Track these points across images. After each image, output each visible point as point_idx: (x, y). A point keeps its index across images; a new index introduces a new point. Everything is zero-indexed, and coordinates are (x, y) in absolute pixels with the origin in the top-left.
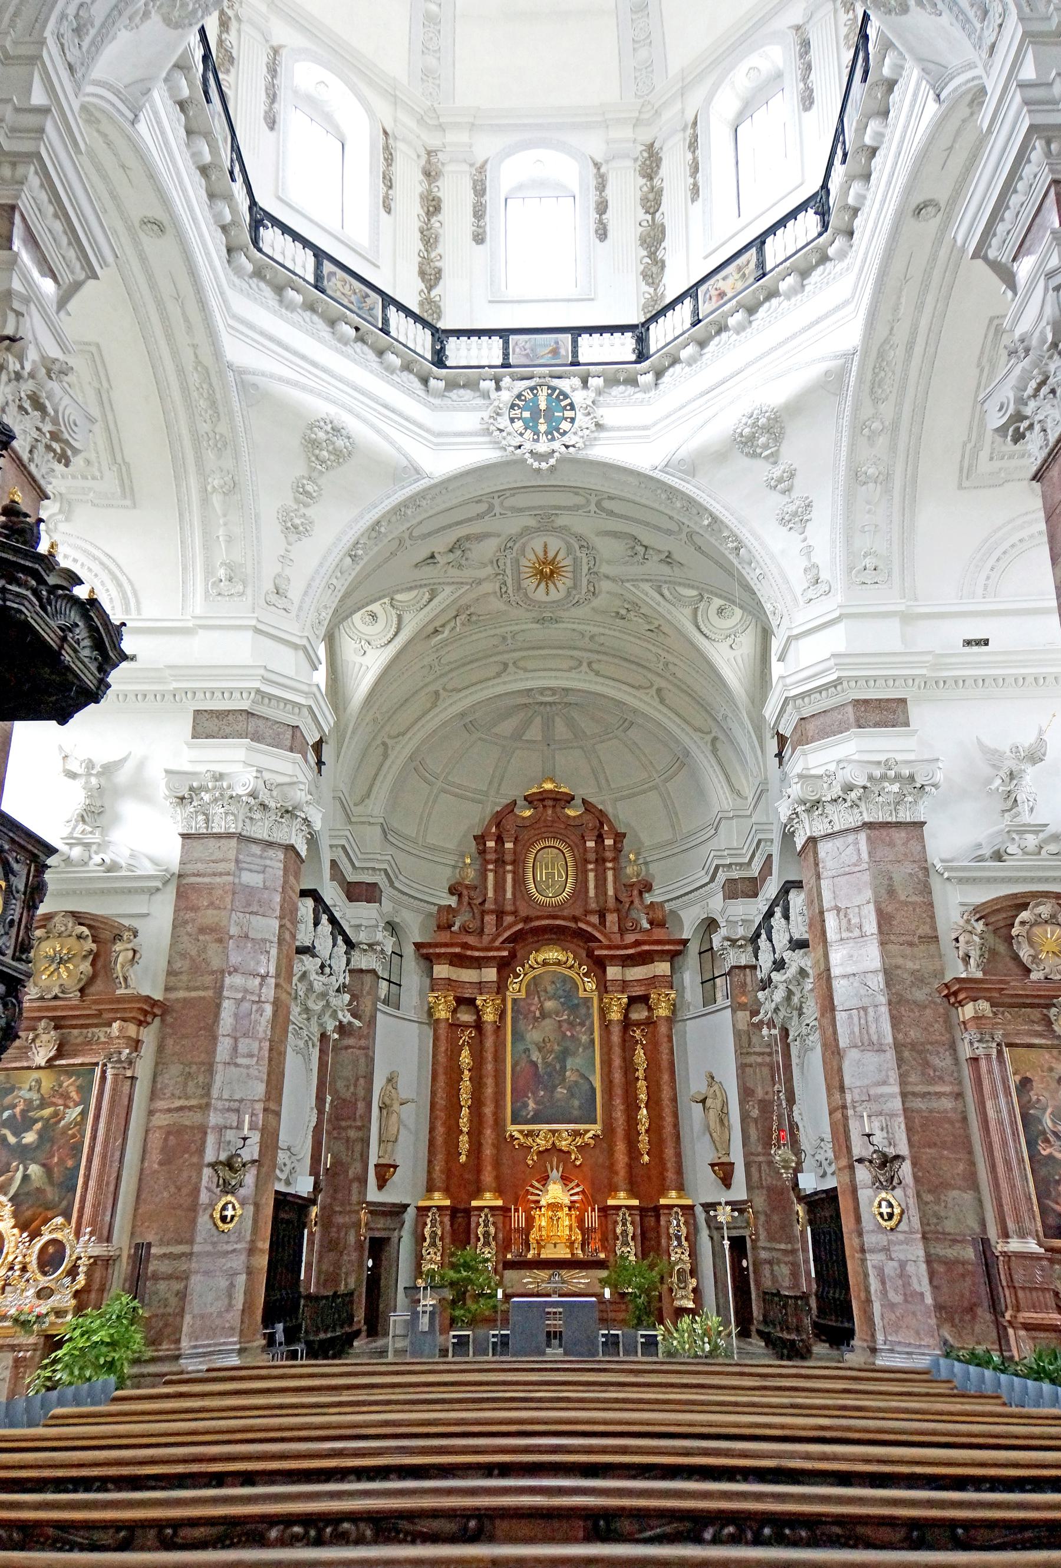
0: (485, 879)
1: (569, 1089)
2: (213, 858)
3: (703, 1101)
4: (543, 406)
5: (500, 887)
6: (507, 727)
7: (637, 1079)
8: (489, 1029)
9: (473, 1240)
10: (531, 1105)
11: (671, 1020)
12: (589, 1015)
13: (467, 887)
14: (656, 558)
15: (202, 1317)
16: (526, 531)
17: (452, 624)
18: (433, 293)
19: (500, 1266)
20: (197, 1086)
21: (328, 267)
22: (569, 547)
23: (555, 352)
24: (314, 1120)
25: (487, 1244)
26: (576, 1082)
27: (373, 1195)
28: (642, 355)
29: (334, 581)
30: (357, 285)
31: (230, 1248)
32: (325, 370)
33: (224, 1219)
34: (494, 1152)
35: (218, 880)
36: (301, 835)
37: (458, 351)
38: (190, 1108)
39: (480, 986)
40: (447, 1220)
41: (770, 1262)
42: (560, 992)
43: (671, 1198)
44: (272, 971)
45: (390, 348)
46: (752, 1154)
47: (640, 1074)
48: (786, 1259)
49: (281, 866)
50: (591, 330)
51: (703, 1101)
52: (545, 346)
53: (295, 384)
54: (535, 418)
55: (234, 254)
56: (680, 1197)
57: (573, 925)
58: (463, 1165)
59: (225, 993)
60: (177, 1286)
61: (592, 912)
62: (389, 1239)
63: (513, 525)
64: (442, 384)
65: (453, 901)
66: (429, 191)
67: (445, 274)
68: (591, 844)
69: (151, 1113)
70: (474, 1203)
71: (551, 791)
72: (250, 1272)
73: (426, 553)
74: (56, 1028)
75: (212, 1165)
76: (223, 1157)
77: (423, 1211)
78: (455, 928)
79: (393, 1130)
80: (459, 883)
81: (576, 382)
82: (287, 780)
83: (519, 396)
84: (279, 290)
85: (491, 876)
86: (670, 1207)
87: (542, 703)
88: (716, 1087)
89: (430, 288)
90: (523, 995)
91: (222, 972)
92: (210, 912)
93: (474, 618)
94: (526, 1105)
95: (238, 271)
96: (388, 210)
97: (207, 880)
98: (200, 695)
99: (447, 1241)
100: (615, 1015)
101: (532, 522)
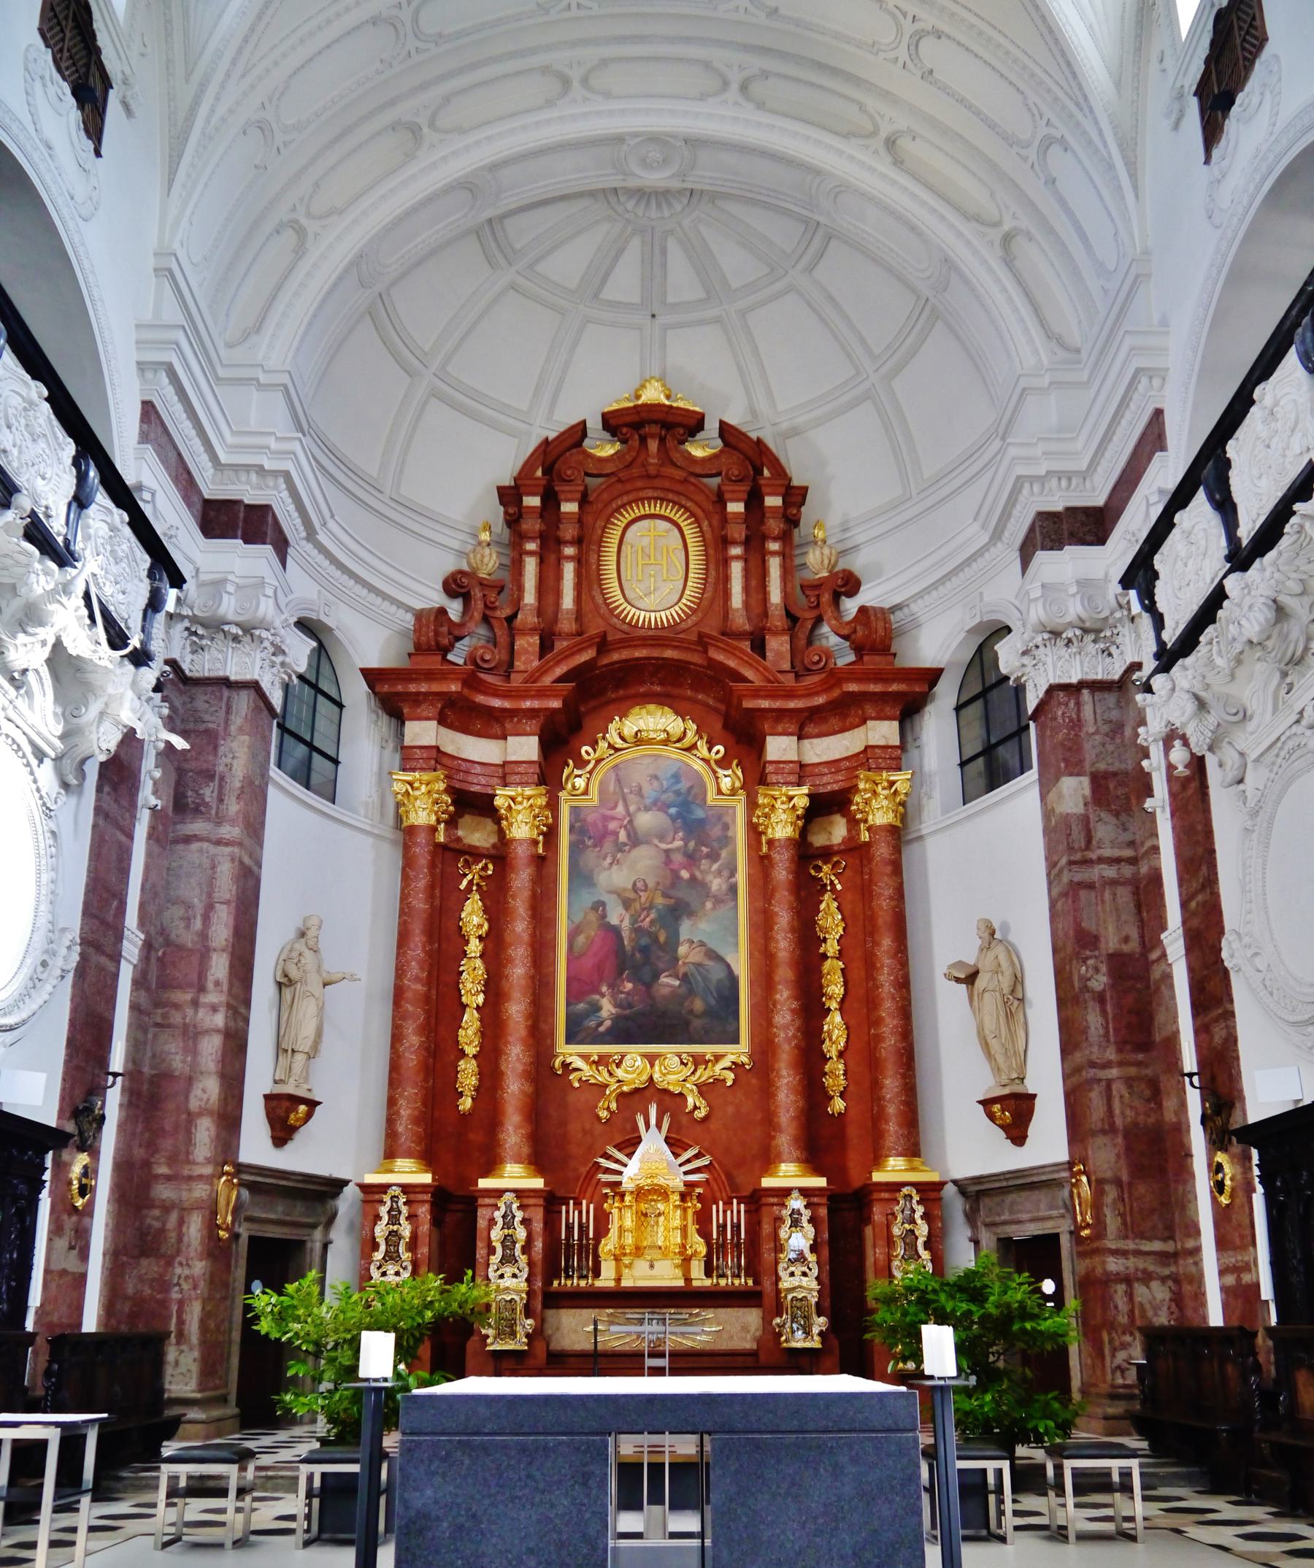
0: (517, 568)
1: (685, 978)
3: (971, 979)
5: (549, 586)
8: (522, 852)
9: (481, 1252)
11: (898, 834)
12: (727, 840)
13: (482, 584)
19: (538, 1304)
25: (508, 1259)
26: (698, 965)
34: (528, 1088)
39: (505, 773)
40: (424, 1211)
41: (1128, 1280)
42: (669, 797)
43: (894, 1169)
46: (1093, 1065)
47: (831, 947)
48: (1166, 1272)
51: (971, 979)
56: (913, 1169)
57: (696, 658)
58: (465, 1117)
61: (740, 635)
62: (303, 1242)
65: (454, 609)
68: (735, 507)
70: (484, 1183)
71: (660, 406)
77: (372, 1193)
79: (306, 1032)
80: (461, 572)
85: (531, 565)
86: (897, 1187)
88: (999, 951)
94: (599, 1009)
99: (424, 1250)
100: (782, 828)
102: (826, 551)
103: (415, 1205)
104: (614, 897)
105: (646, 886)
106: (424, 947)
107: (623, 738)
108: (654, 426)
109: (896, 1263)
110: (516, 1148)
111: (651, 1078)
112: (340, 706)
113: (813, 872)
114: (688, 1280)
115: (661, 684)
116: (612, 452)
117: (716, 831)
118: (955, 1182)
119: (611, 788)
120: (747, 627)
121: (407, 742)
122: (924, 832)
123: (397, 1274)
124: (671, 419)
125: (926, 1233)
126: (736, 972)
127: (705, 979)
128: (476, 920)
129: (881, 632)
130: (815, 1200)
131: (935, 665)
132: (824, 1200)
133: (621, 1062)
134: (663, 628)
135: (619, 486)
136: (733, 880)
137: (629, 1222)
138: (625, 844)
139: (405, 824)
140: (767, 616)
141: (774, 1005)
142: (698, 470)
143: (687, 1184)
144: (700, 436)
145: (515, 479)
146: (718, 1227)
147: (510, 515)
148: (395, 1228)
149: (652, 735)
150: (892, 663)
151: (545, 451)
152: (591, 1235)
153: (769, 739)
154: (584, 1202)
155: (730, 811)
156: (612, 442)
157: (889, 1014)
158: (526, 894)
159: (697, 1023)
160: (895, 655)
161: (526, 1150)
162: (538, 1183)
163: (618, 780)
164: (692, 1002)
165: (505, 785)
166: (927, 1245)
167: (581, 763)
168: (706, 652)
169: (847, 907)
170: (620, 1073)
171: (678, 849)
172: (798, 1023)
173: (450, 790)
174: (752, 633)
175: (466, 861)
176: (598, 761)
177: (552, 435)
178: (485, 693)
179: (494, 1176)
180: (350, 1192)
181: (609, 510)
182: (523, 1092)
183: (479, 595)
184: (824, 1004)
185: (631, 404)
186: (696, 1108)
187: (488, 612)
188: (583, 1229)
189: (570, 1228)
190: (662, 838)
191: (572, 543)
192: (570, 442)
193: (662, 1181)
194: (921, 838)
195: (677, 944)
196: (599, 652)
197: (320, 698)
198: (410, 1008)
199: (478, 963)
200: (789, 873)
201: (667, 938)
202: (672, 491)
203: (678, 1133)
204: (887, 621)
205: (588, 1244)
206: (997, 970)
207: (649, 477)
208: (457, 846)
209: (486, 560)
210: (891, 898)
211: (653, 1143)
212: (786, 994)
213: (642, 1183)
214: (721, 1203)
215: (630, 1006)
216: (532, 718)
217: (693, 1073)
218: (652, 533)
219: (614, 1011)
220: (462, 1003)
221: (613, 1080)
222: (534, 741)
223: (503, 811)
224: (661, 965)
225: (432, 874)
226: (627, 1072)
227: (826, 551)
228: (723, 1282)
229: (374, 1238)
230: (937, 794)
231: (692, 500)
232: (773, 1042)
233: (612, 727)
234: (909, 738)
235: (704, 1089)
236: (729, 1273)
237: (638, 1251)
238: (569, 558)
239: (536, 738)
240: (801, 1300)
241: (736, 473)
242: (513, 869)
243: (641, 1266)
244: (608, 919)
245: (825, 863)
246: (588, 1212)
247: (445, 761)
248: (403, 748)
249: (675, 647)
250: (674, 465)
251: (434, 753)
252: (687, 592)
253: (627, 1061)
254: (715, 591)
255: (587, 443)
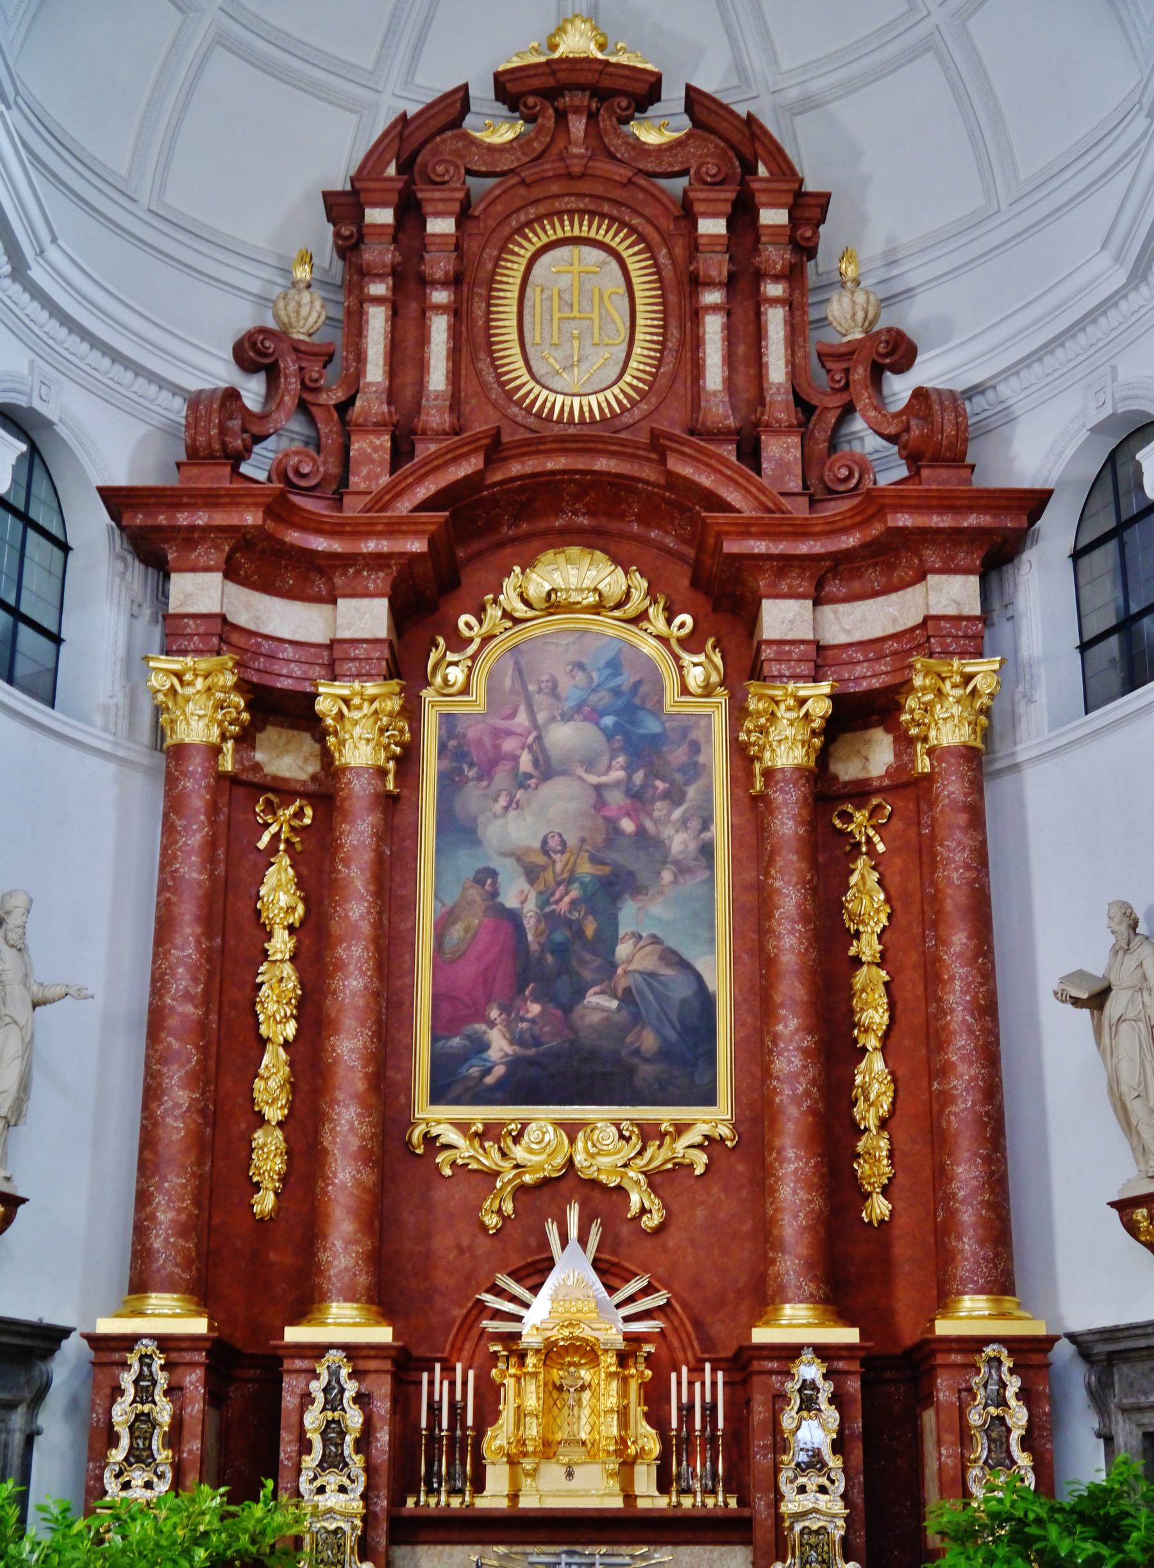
0: (355, 324)
1: (627, 998)
7: (857, 962)
8: (359, 789)
9: (287, 1448)
10: (499, 1046)
12: (695, 770)
13: (297, 349)
25: (332, 1461)
34: (368, 1177)
40: (194, 1380)
42: (603, 698)
56: (1003, 1315)
57: (649, 473)
61: (718, 435)
68: (712, 227)
70: (293, 1334)
80: (264, 331)
85: (377, 320)
86: (975, 1344)
94: (482, 1046)
99: (193, 1446)
102: (860, 298)
103: (179, 1371)
104: (510, 862)
105: (563, 843)
106: (198, 942)
107: (527, 603)
108: (579, 94)
109: (975, 1472)
110: (347, 1277)
111: (570, 1161)
112: (64, 548)
113: (838, 823)
115: (590, 513)
116: (510, 136)
117: (678, 755)
118: (1072, 1337)
119: (508, 683)
120: (731, 422)
121: (174, 607)
122: (1020, 758)
123: (148, 1485)
124: (606, 82)
125: (1024, 1422)
126: (711, 988)
127: (660, 998)
128: (284, 899)
129: (950, 430)
130: (841, 1365)
131: (1038, 486)
132: (855, 1366)
133: (521, 1134)
134: (593, 422)
135: (522, 191)
136: (706, 835)
137: (532, 1401)
138: (529, 776)
139: (169, 742)
140: (763, 405)
141: (775, 1043)
142: (651, 167)
143: (629, 1337)
144: (653, 110)
145: (353, 180)
146: (680, 1408)
147: (344, 238)
148: (146, 1408)
149: (575, 597)
150: (969, 481)
151: (401, 134)
152: (470, 1422)
153: (766, 604)
154: (459, 1367)
155: (703, 723)
156: (511, 121)
157: (962, 1059)
158: (367, 856)
159: (646, 1071)
160: (973, 467)
161: (363, 1280)
162: (383, 1334)
163: (519, 670)
164: (639, 1036)
165: (334, 678)
166: (1026, 1443)
167: (458, 643)
168: (663, 461)
169: (894, 881)
170: (518, 1153)
171: (617, 784)
172: (812, 1072)
173: (242, 686)
174: (738, 432)
175: (268, 802)
176: (486, 639)
177: (413, 109)
178: (303, 528)
179: (309, 1323)
180: (73, 1349)
181: (506, 231)
182: (359, 1184)
183: (293, 368)
184: (856, 1041)
185: (543, 59)
186: (644, 1211)
187: (307, 396)
190: (590, 765)
191: (444, 284)
192: (442, 120)
193: (587, 1333)
194: (1015, 768)
195: (614, 940)
196: (488, 462)
197: (31, 534)
198: (176, 1045)
199: (288, 970)
200: (799, 824)
201: (598, 932)
202: (610, 200)
203: (614, 1252)
204: (959, 412)
205: (465, 1437)
207: (570, 176)
208: (256, 779)
209: (304, 311)
210: (967, 867)
212: (793, 1023)
213: (555, 1334)
214: (684, 1369)
215: (537, 1042)
216: (381, 568)
217: (640, 1153)
218: (576, 268)
219: (509, 1049)
220: (261, 1036)
221: (507, 1165)
222: (381, 606)
223: (329, 721)
224: (587, 975)
225: (212, 824)
226: (531, 1151)
227: (860, 298)
228: (687, 1502)
229: (110, 1426)
230: (1041, 696)
231: (640, 214)
232: (772, 1102)
233: (509, 584)
234: (996, 605)
235: (658, 1179)
236: (697, 1486)
237: (548, 1449)
238: (440, 308)
239: (385, 602)
240: (817, 1532)
241: (714, 171)
242: (345, 815)
243: (552, 1474)
244: (500, 899)
245: (858, 808)
246: (465, 1383)
247: (235, 638)
248: (167, 616)
249: (613, 454)
250: (613, 157)
251: (217, 626)
252: (633, 364)
254: (679, 360)
255: (469, 121)
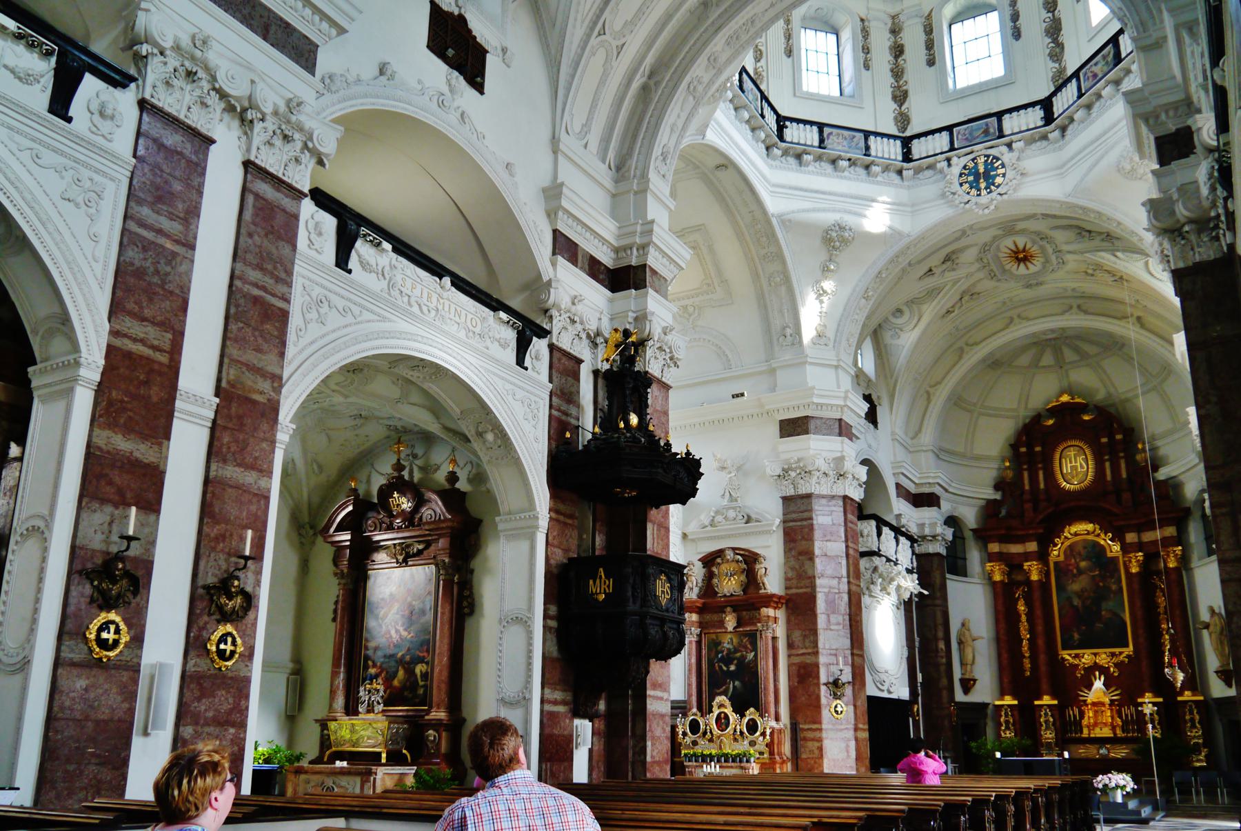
2: (802, 509)
4: (982, 169)
5: (1034, 480)
6: (1025, 360)
7: (1159, 614)
10: (1076, 636)
12: (1119, 571)
14: (1099, 238)
15: (834, 760)
16: (995, 238)
17: (959, 304)
18: (903, 108)
20: (810, 642)
21: (827, 130)
22: (1034, 242)
23: (986, 132)
24: (906, 654)
25: (1047, 728)
27: (960, 696)
28: (1049, 118)
29: (856, 317)
30: (846, 133)
31: (843, 727)
32: (830, 194)
33: (837, 712)
35: (805, 523)
36: (852, 488)
37: (918, 148)
38: (809, 654)
39: (1027, 556)
40: (1016, 713)
44: (844, 572)
45: (872, 163)
49: (842, 509)
50: (1010, 111)
52: (979, 129)
53: (814, 210)
54: (977, 179)
55: (770, 150)
59: (818, 589)
60: (817, 744)
63: (986, 237)
64: (911, 172)
65: (998, 496)
66: (895, 42)
67: (911, 93)
69: (789, 656)
70: (1037, 703)
72: (856, 739)
73: (926, 269)
74: (734, 611)
75: (825, 684)
76: (831, 680)
78: (1003, 512)
79: (970, 657)
81: (1004, 149)
82: (839, 455)
83: (964, 168)
84: (798, 157)
85: (1026, 474)
87: (1047, 340)
89: (900, 106)
90: (1062, 558)
91: (814, 577)
92: (804, 542)
93: (974, 297)
95: (774, 159)
96: (867, 67)
97: (799, 523)
98: (781, 411)
101: (1000, 232)
114: (1115, 734)
137: (1091, 715)
162: (1055, 702)
165: (1027, 561)
170: (1083, 660)
180: (991, 706)
188: (1075, 716)
189: (1070, 716)
193: (1102, 700)
206: (1216, 625)
211: (1098, 684)
233: (1066, 530)
237: (1096, 724)
243: (1097, 730)
253: (1086, 656)
